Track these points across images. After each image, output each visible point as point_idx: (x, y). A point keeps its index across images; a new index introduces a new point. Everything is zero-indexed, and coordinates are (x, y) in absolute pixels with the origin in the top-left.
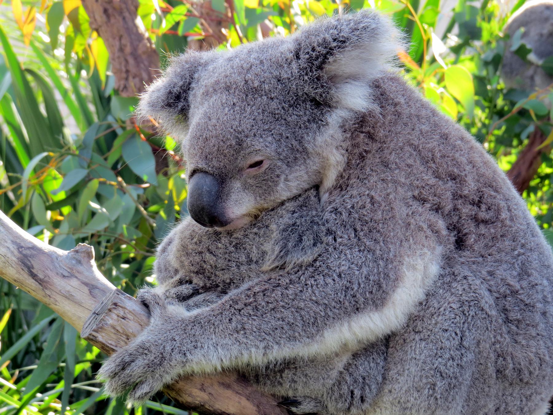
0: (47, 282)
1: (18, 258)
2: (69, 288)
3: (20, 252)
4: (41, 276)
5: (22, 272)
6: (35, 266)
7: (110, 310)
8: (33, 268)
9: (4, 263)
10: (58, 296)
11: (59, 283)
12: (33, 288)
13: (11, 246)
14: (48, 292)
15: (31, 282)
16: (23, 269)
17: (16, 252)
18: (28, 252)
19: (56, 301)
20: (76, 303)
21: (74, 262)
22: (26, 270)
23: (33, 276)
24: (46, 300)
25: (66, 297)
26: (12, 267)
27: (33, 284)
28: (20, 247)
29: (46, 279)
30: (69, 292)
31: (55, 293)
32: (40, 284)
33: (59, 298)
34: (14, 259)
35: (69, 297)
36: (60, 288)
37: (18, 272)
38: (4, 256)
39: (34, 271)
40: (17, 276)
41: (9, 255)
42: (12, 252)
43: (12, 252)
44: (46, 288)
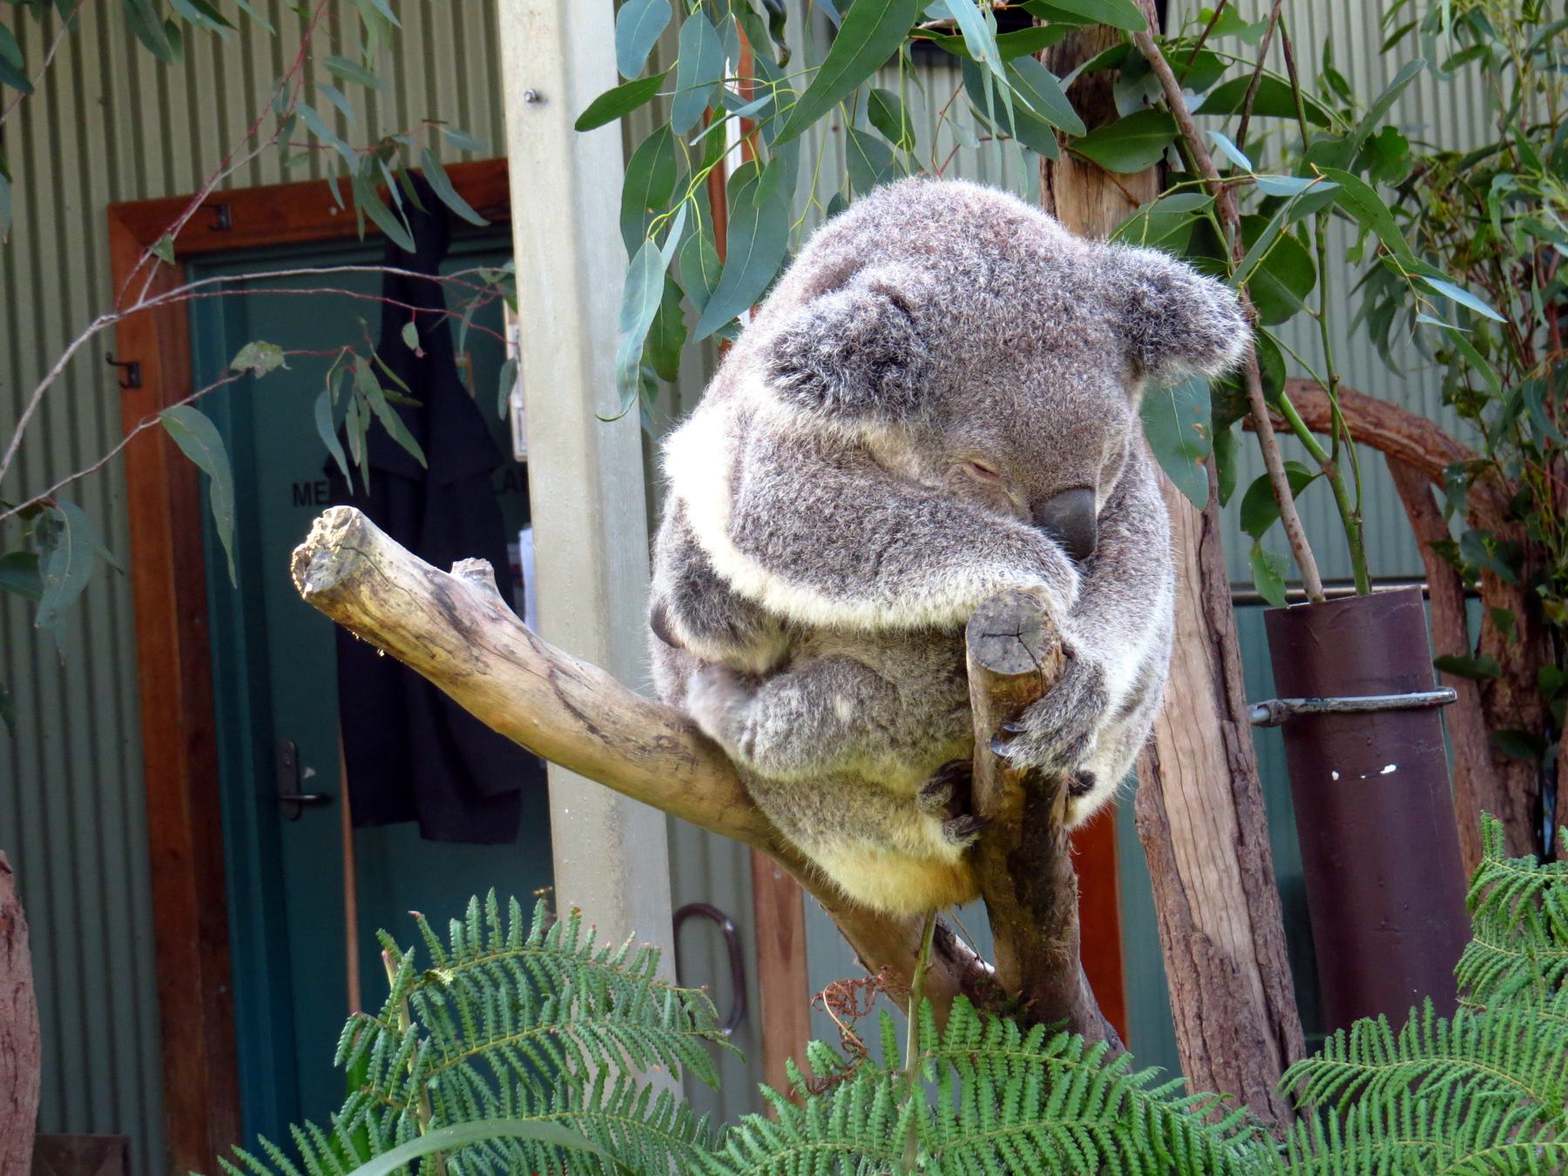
0: (476, 632)
1: (432, 593)
2: (506, 640)
3: (431, 581)
4: (467, 623)
5: (439, 619)
6: (458, 604)
7: (1045, 623)
8: (455, 609)
9: (409, 604)
10: (492, 656)
11: (488, 628)
12: (450, 647)
13: (419, 574)
14: (476, 652)
15: (451, 637)
16: (440, 613)
17: (426, 583)
18: (437, 580)
19: (488, 666)
20: (519, 665)
21: (489, 592)
22: (445, 613)
23: (456, 623)
24: (466, 667)
25: (506, 658)
26: (422, 610)
27: (454, 640)
28: (426, 573)
29: (474, 627)
30: (506, 646)
31: (485, 652)
32: (465, 637)
33: (491, 660)
34: (427, 596)
35: (508, 656)
36: (494, 642)
37: (432, 619)
38: (409, 592)
39: (457, 614)
40: (429, 627)
41: (417, 589)
42: (420, 583)
43: (420, 583)
44: (474, 645)
